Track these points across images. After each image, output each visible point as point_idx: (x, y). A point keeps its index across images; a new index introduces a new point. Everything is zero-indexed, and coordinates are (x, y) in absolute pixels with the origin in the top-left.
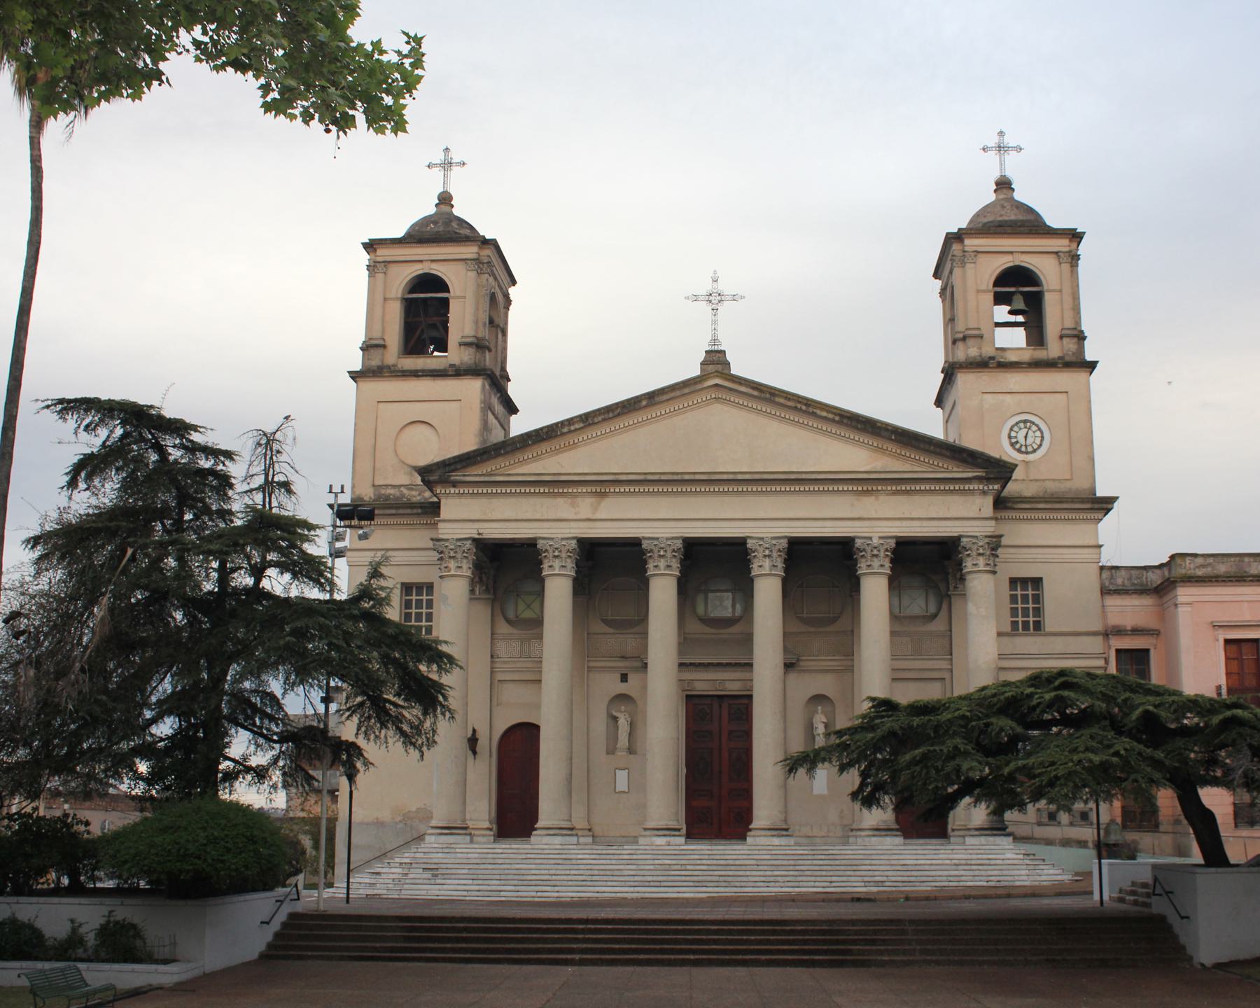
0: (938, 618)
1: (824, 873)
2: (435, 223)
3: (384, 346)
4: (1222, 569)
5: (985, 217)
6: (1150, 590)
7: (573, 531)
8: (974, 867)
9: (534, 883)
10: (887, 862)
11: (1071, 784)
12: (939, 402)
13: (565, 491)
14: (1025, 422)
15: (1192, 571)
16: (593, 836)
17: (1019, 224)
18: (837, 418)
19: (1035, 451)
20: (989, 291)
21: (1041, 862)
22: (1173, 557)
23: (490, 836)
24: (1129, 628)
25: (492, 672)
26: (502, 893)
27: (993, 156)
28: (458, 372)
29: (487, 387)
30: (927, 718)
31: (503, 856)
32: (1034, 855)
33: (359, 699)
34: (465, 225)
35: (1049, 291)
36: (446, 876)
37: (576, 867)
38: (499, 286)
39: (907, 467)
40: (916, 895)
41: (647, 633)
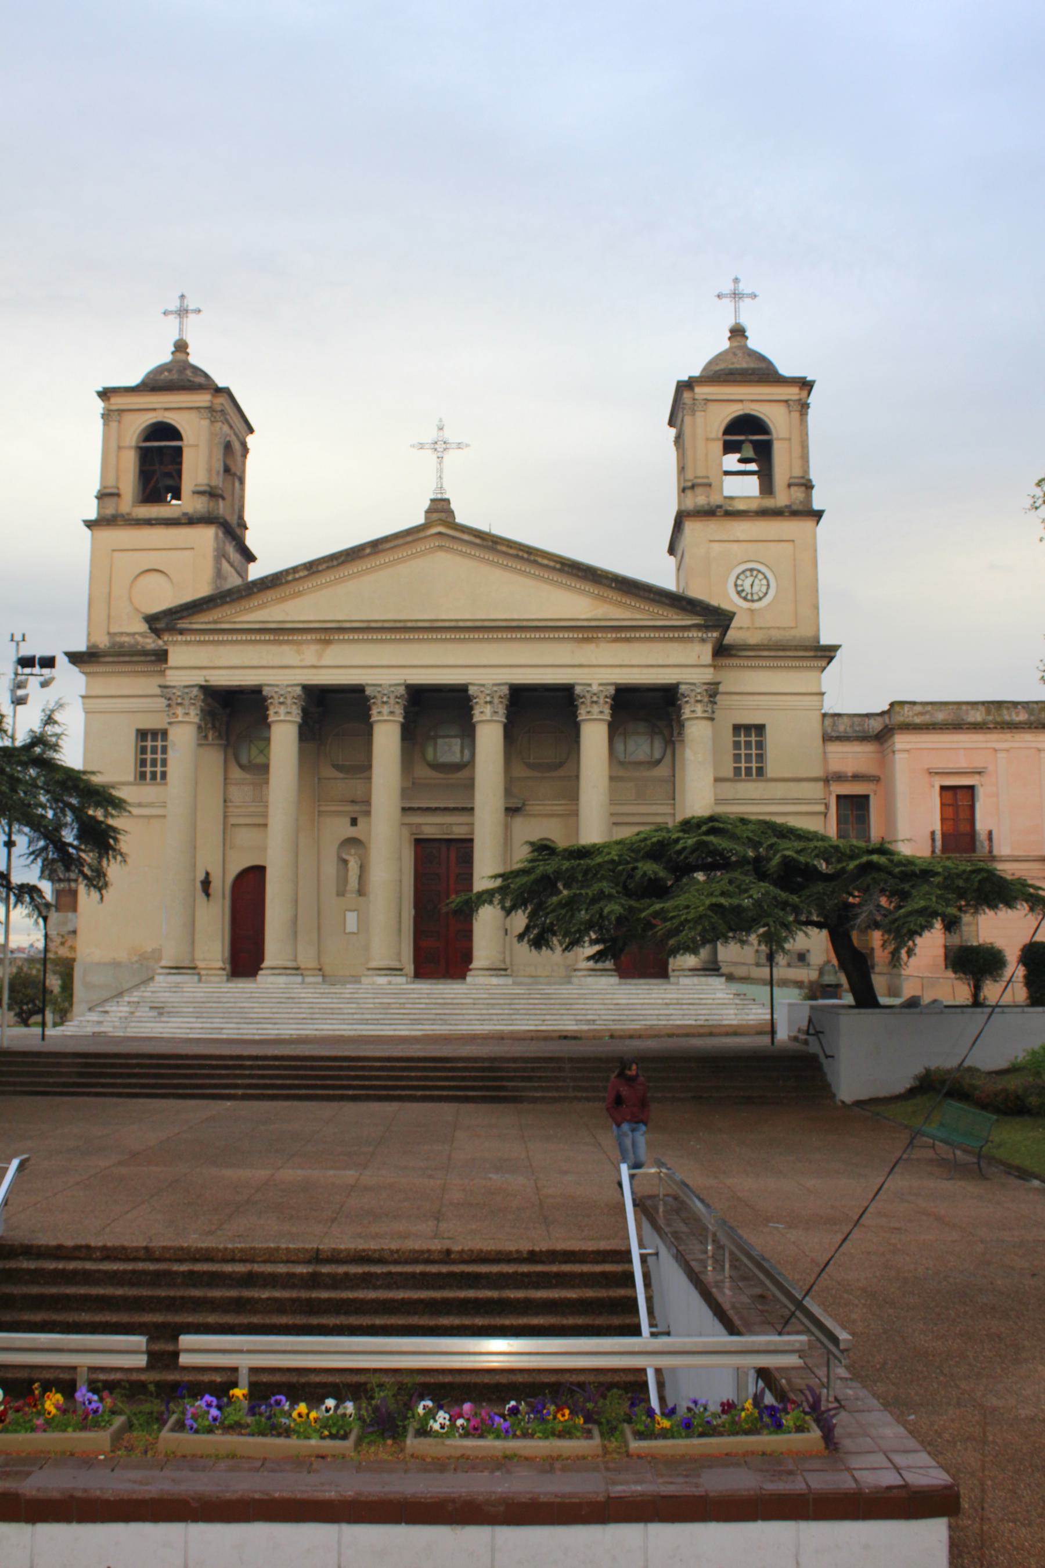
0: (661, 764)
1: (538, 1012)
2: (170, 371)
3: (118, 495)
4: (940, 716)
5: (717, 364)
6: (870, 737)
7: (298, 677)
8: (685, 1007)
9: (255, 1021)
10: (601, 1001)
11: (700, 928)
12: (672, 551)
13: (290, 638)
14: (751, 570)
15: (911, 719)
16: (324, 976)
17: (750, 372)
18: (558, 566)
19: (760, 599)
20: (717, 439)
21: (752, 1002)
22: (892, 705)
23: (222, 975)
24: (850, 774)
25: (225, 817)
26: (224, 1031)
27: (728, 304)
28: (191, 521)
29: (221, 535)
30: (578, 862)
31: (228, 995)
32: (745, 995)
33: (42, 843)
34: (199, 373)
35: (779, 439)
36: (171, 1015)
37: (298, 1005)
38: (236, 434)
39: (628, 614)
40: (622, 1033)
41: (370, 778)
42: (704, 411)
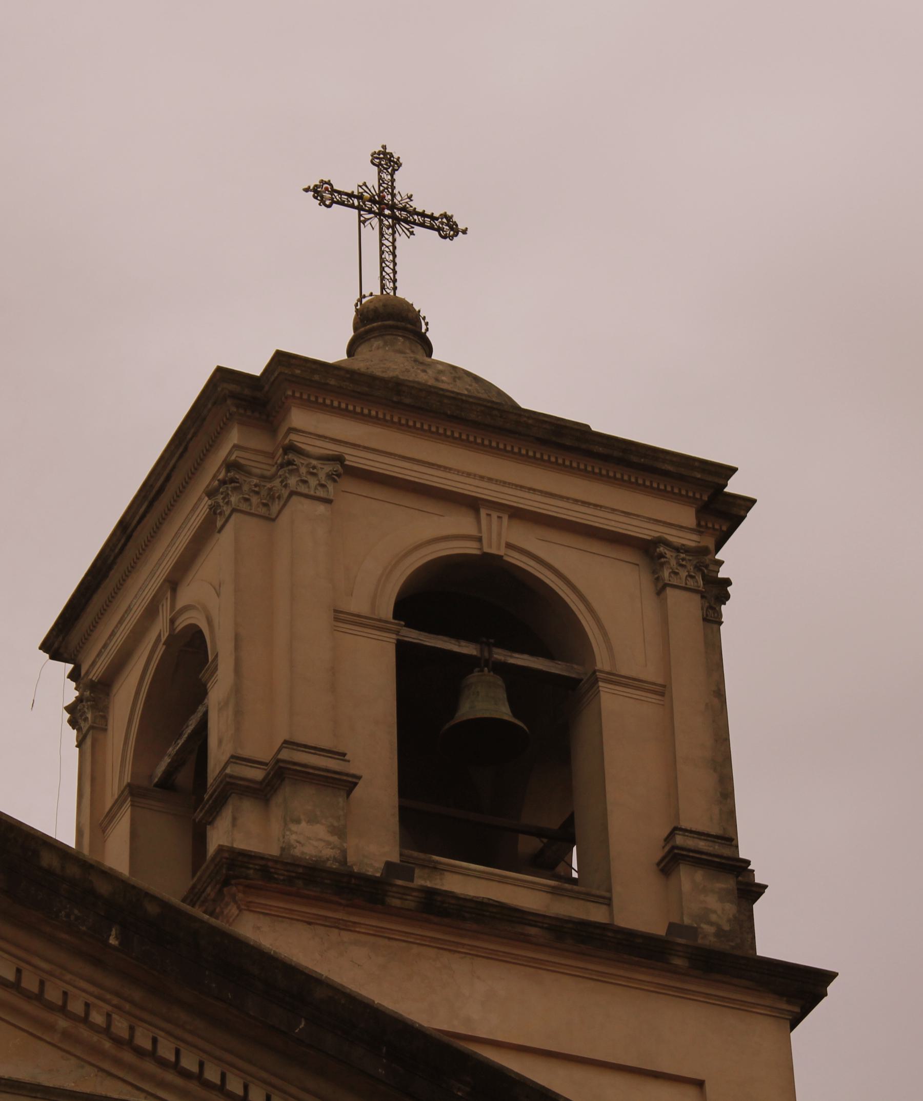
42: (328, 501)
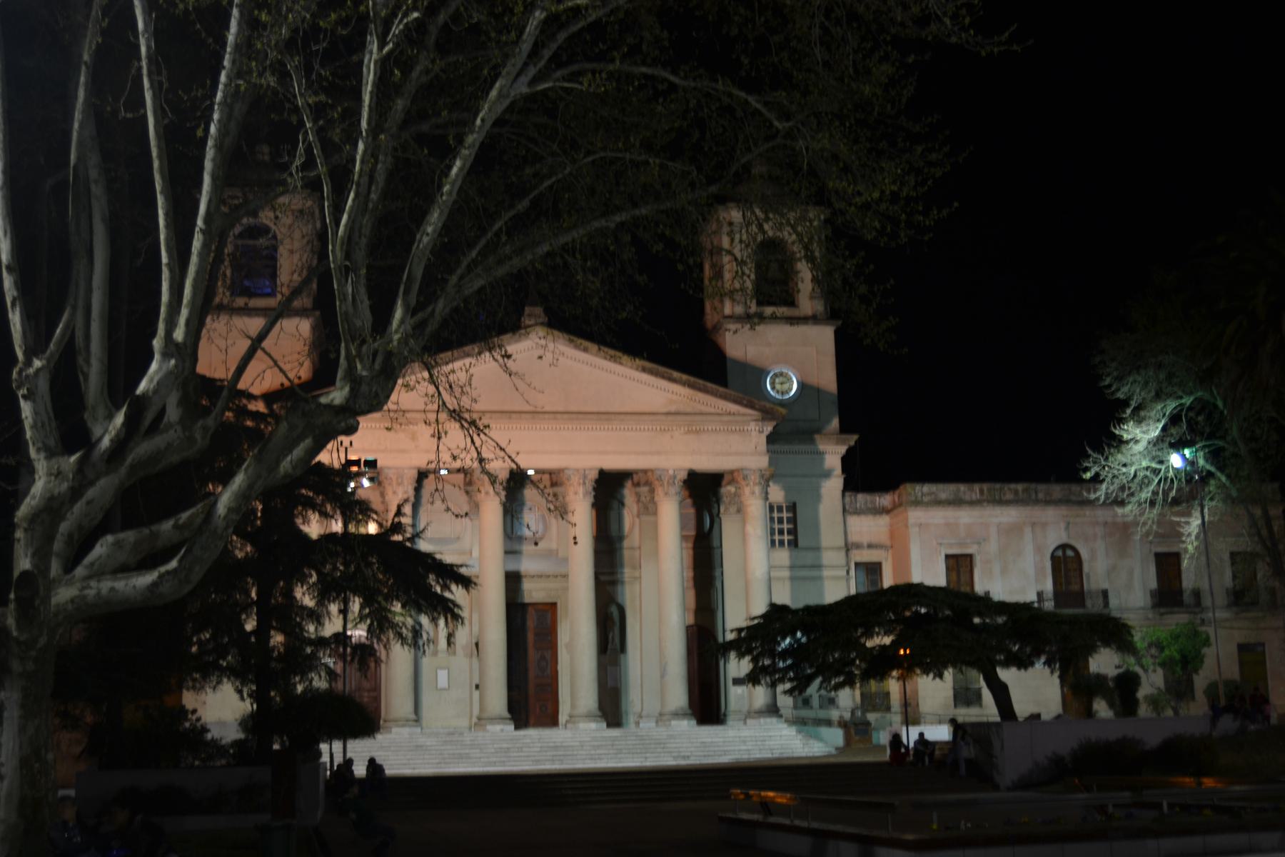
24: (865, 544)
